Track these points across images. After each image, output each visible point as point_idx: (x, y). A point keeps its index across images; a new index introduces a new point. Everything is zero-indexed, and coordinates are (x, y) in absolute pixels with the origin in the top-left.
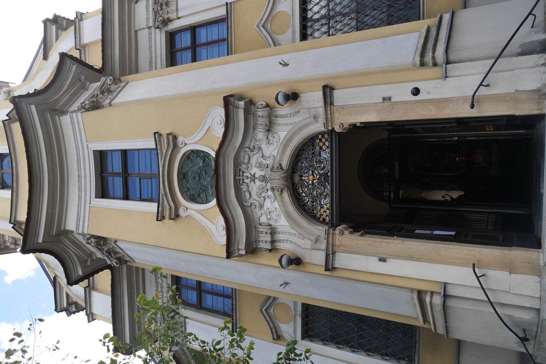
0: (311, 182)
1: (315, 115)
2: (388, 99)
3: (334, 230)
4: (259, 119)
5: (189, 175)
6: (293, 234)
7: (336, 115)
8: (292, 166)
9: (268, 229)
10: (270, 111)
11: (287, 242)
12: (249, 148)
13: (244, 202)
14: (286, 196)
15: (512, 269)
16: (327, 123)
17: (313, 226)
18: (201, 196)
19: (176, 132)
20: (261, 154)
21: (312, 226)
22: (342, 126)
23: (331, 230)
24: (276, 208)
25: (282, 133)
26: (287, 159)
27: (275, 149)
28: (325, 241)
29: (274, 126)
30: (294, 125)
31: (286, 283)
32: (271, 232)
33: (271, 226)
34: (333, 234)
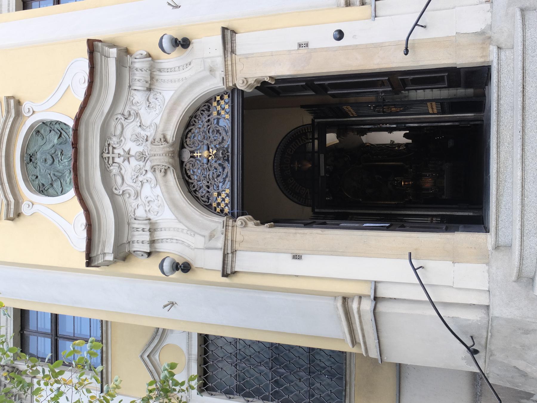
0: (205, 161)
1: (211, 67)
2: (305, 45)
3: (235, 221)
4: (136, 72)
5: (38, 157)
6: (180, 230)
7: (239, 67)
8: (181, 139)
9: (146, 224)
10: (152, 62)
11: (172, 242)
12: (123, 115)
13: (114, 190)
14: (172, 179)
16: (226, 77)
17: (207, 218)
18: (54, 186)
19: (20, 95)
20: (139, 122)
21: (205, 217)
22: (245, 82)
23: (231, 220)
24: (158, 196)
26: (173, 128)
27: (158, 114)
28: (223, 236)
29: (156, 84)
30: (184, 81)
31: (172, 304)
32: (150, 229)
33: (150, 221)
34: (232, 227)
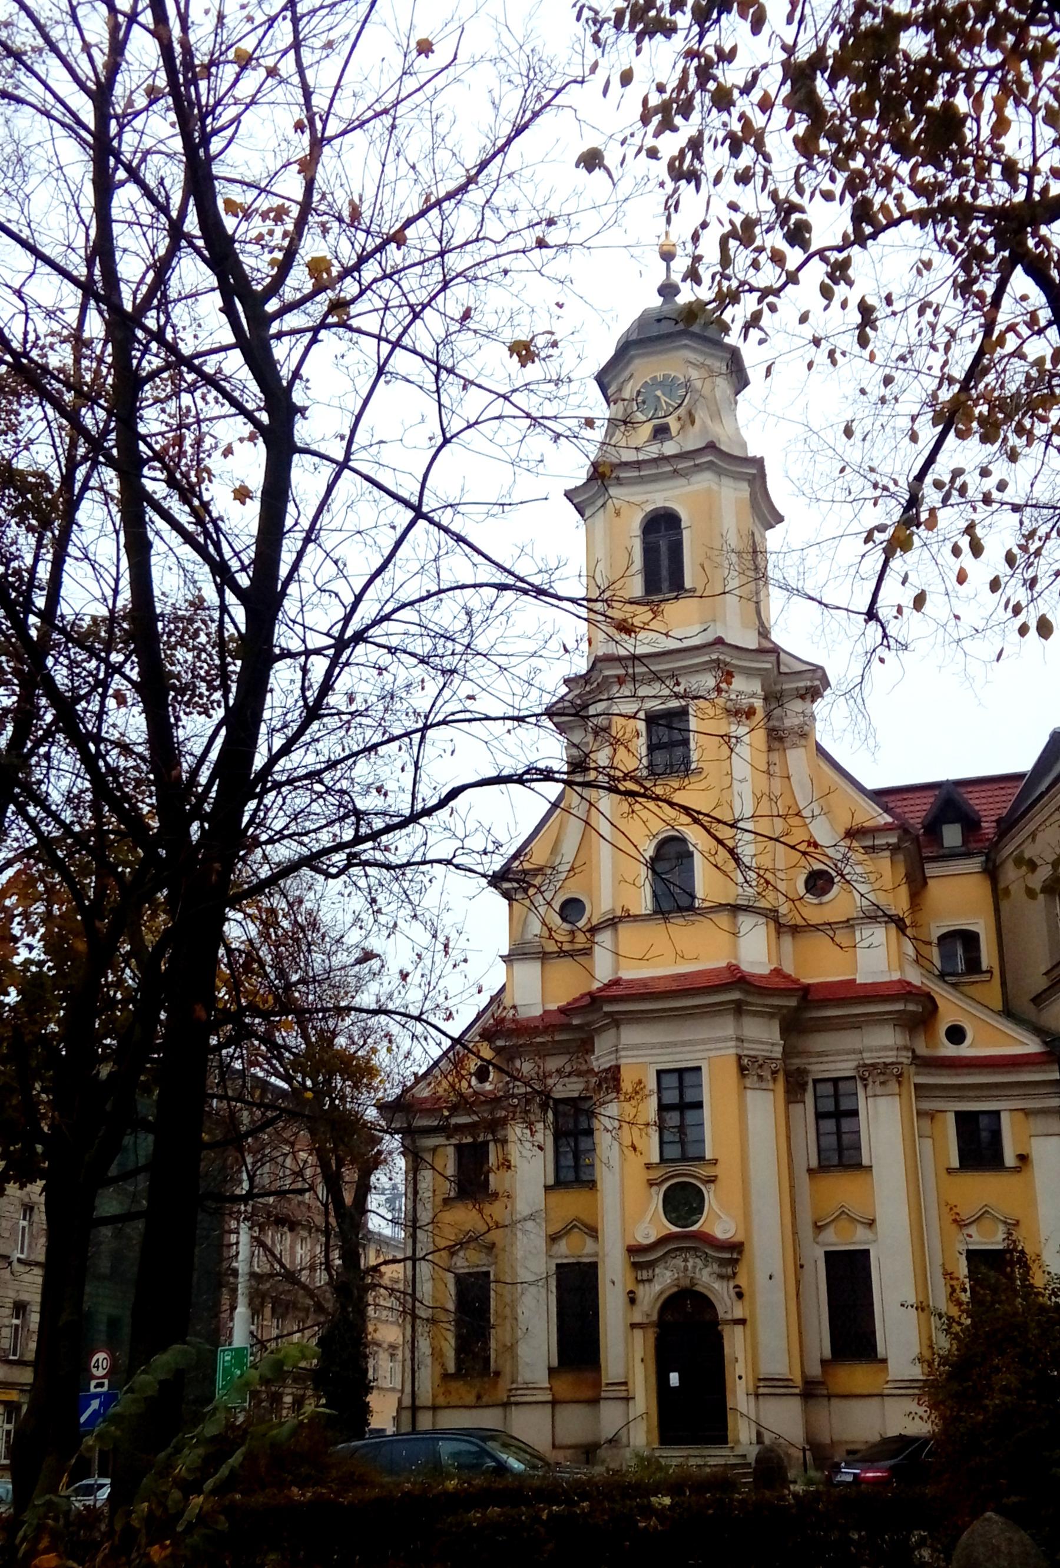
14: (675, 1289)
15: (648, 1432)
19: (718, 1182)
25: (717, 1285)
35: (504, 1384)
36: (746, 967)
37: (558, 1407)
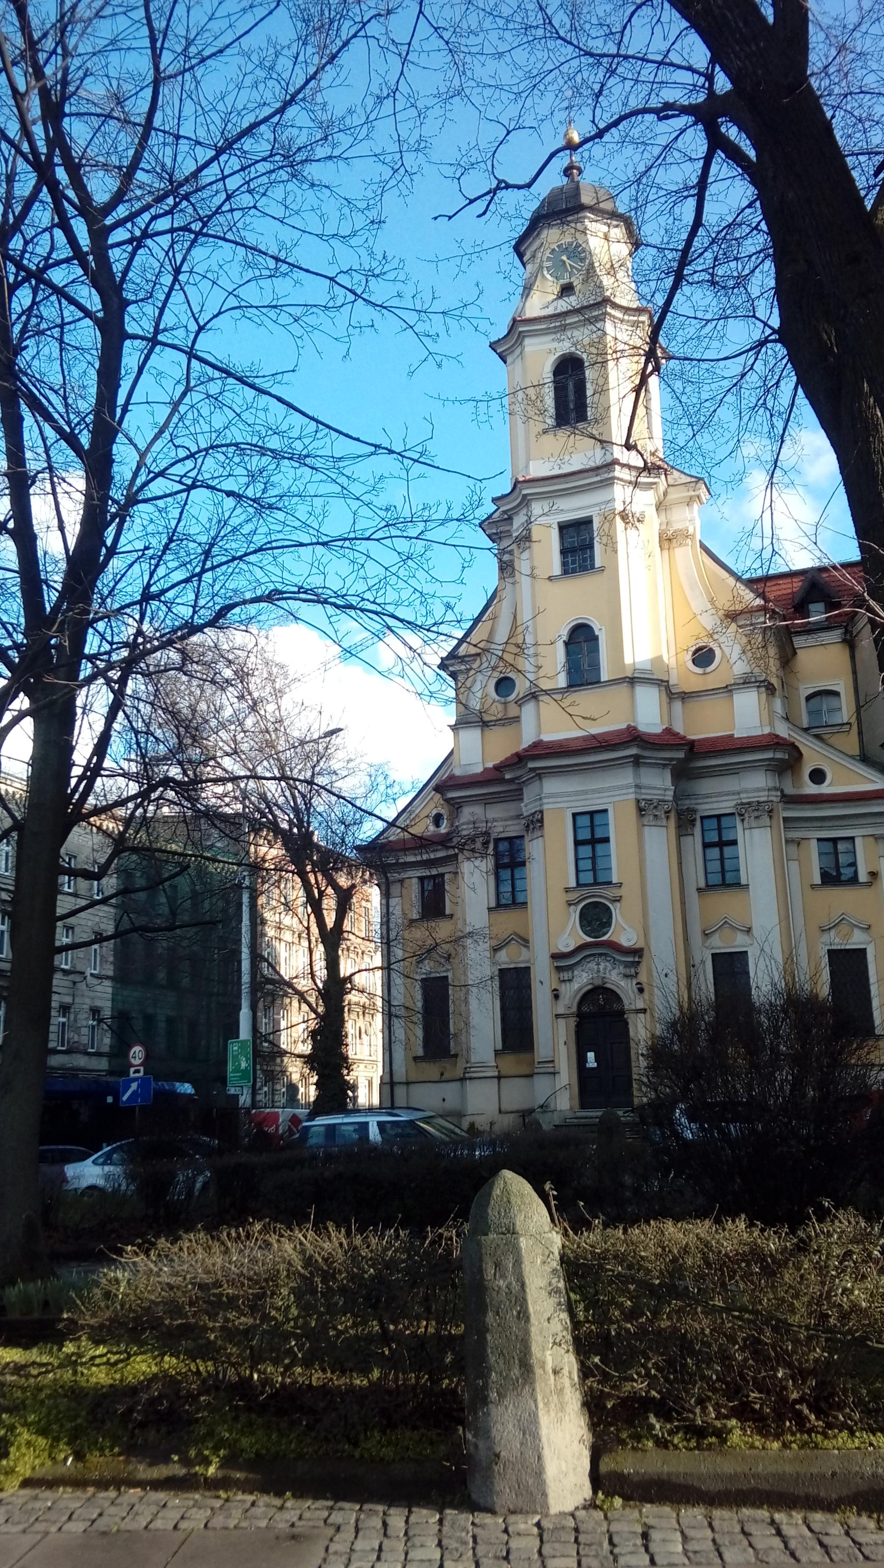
14: (590, 987)
15: (571, 1099)
35: (461, 1064)
36: (642, 728)
37: (502, 1080)
